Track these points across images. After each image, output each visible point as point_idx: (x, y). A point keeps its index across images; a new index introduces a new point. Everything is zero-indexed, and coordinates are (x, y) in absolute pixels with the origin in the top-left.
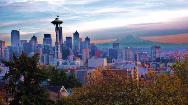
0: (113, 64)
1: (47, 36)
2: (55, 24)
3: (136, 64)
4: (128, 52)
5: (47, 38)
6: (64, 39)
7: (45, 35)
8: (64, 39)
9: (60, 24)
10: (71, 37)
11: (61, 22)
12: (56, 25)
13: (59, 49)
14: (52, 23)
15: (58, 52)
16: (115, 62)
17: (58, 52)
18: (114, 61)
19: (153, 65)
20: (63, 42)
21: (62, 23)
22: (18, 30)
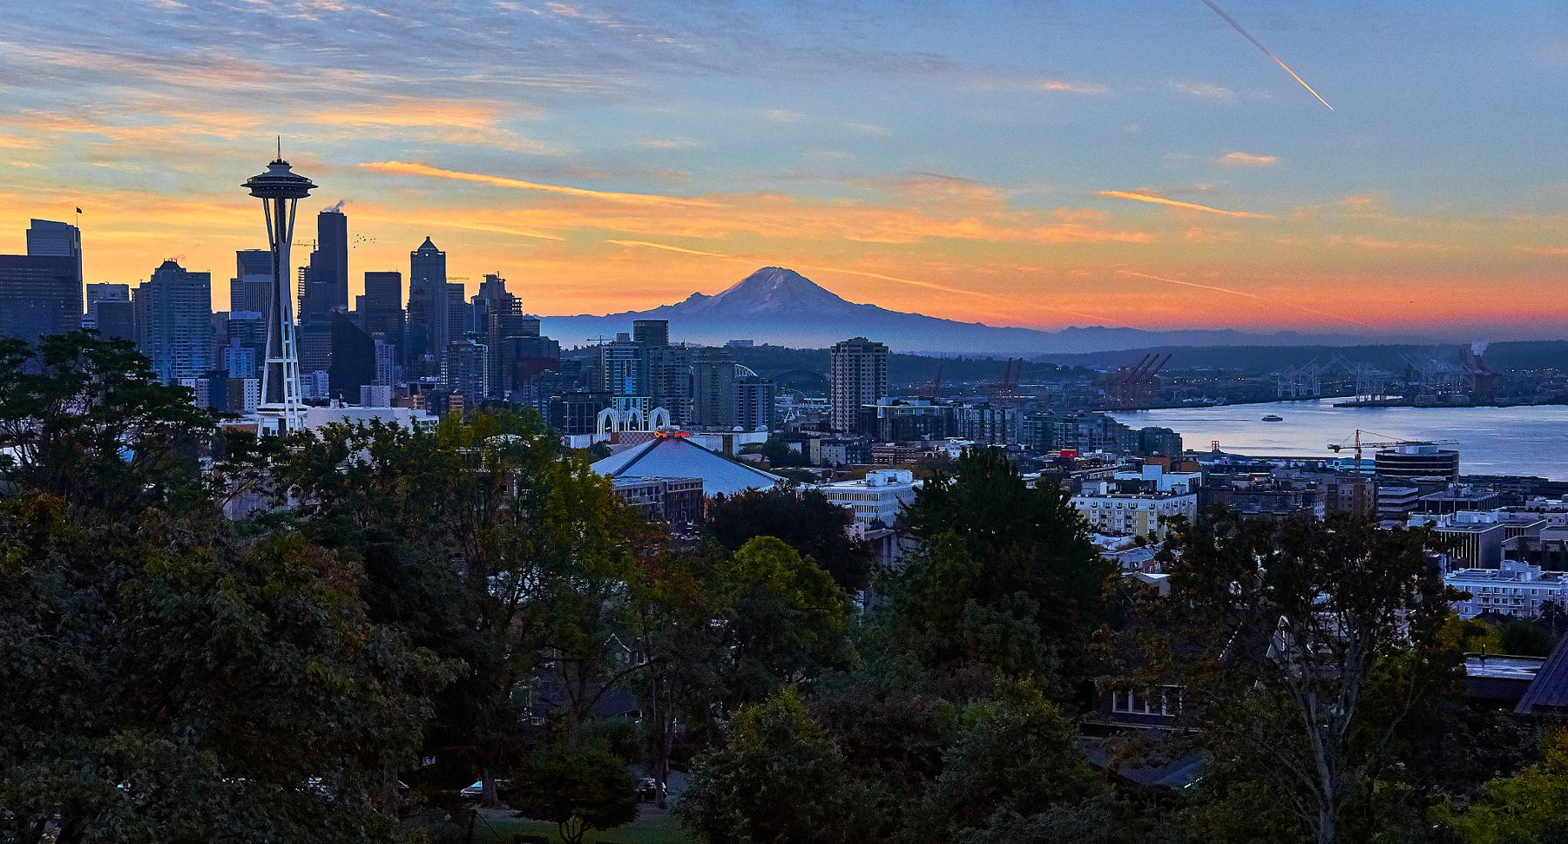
3: (728, 442)
6: (356, 288)
8: (356, 288)
9: (295, 197)
10: (397, 276)
11: (300, 188)
12: (271, 201)
13: (289, 342)
14: (250, 190)
15: (281, 365)
16: (616, 429)
17: (281, 365)
19: (826, 449)
20: (352, 307)
21: (310, 191)
22: (69, 219)
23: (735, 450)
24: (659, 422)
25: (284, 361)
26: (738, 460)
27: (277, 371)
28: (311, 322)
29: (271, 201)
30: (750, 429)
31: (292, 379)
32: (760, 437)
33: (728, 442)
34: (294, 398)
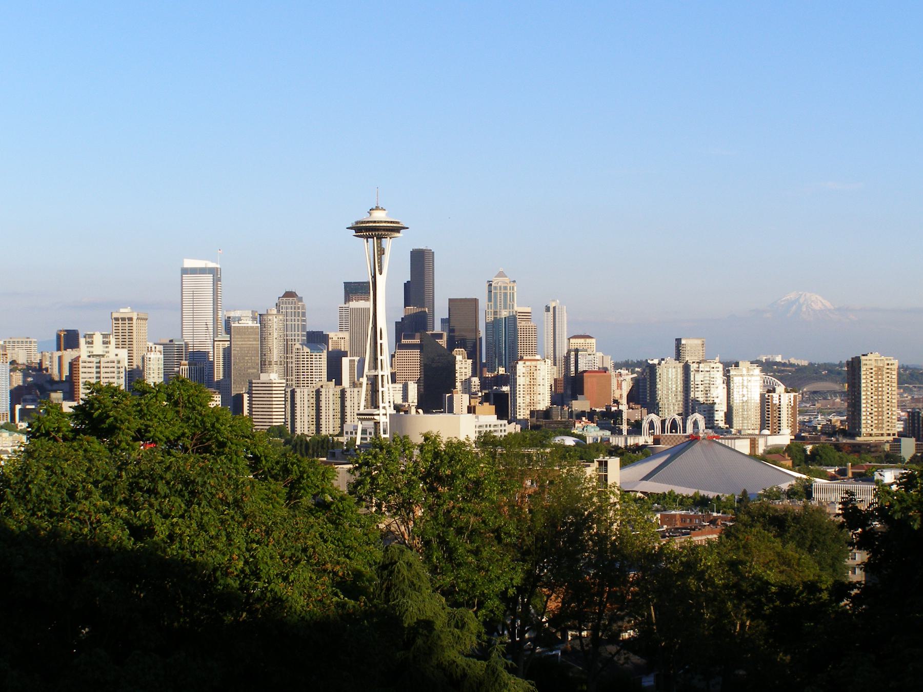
1: (354, 290)
2: (367, 237)
3: (753, 444)
4: (736, 381)
5: (354, 304)
6: (441, 311)
7: (347, 285)
8: (441, 311)
10: (475, 301)
15: (376, 376)
16: (658, 431)
17: (376, 376)
24: (695, 424)
25: (380, 373)
26: (762, 459)
27: (374, 382)
28: (404, 341)
29: (370, 240)
30: (776, 432)
32: (784, 438)
33: (753, 444)
34: (387, 405)
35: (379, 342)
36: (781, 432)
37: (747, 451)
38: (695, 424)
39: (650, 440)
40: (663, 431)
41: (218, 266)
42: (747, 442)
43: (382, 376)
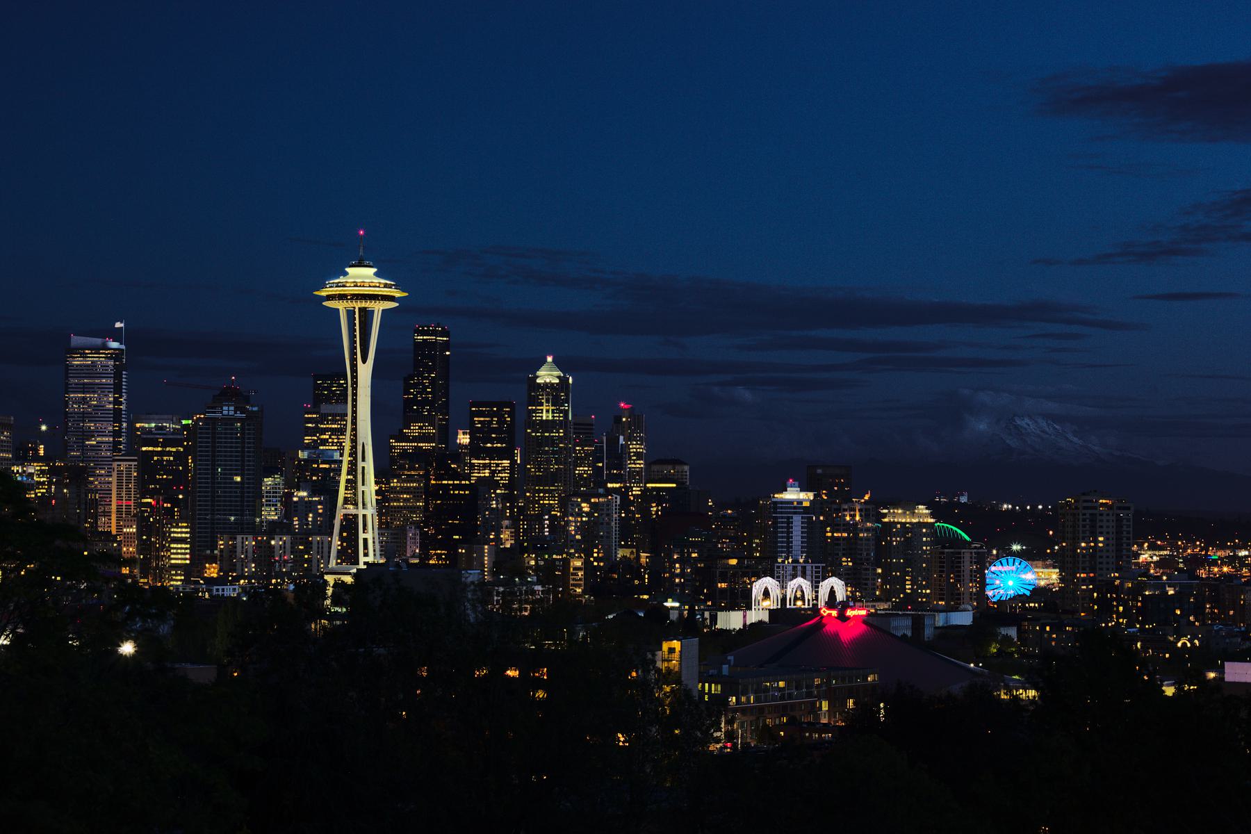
0: (754, 616)
15: (356, 516)
17: (356, 516)
18: (766, 594)
23: (928, 632)
24: (832, 593)
25: (361, 512)
27: (351, 524)
31: (369, 536)
33: (918, 624)
35: (360, 464)
36: (962, 607)
37: (909, 634)
38: (832, 593)
39: (765, 617)
40: (784, 599)
41: (123, 347)
42: (909, 622)
43: (364, 516)
